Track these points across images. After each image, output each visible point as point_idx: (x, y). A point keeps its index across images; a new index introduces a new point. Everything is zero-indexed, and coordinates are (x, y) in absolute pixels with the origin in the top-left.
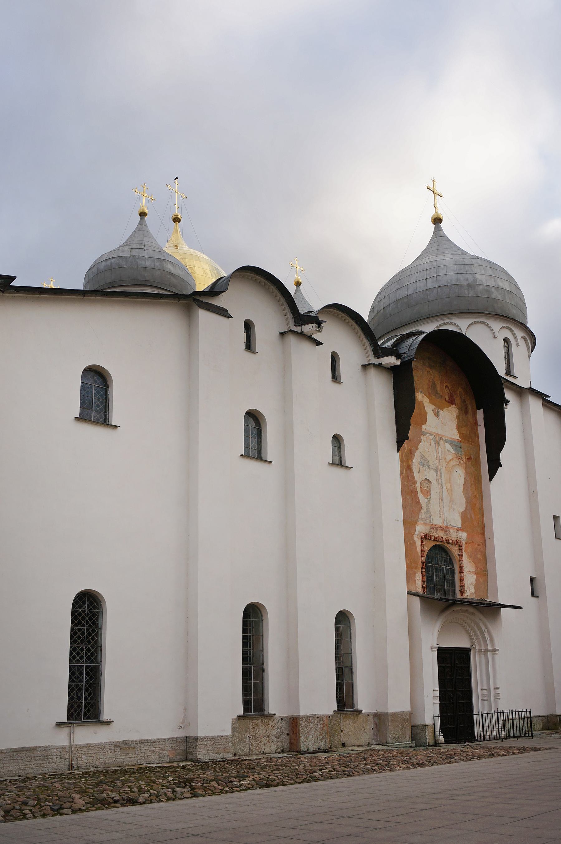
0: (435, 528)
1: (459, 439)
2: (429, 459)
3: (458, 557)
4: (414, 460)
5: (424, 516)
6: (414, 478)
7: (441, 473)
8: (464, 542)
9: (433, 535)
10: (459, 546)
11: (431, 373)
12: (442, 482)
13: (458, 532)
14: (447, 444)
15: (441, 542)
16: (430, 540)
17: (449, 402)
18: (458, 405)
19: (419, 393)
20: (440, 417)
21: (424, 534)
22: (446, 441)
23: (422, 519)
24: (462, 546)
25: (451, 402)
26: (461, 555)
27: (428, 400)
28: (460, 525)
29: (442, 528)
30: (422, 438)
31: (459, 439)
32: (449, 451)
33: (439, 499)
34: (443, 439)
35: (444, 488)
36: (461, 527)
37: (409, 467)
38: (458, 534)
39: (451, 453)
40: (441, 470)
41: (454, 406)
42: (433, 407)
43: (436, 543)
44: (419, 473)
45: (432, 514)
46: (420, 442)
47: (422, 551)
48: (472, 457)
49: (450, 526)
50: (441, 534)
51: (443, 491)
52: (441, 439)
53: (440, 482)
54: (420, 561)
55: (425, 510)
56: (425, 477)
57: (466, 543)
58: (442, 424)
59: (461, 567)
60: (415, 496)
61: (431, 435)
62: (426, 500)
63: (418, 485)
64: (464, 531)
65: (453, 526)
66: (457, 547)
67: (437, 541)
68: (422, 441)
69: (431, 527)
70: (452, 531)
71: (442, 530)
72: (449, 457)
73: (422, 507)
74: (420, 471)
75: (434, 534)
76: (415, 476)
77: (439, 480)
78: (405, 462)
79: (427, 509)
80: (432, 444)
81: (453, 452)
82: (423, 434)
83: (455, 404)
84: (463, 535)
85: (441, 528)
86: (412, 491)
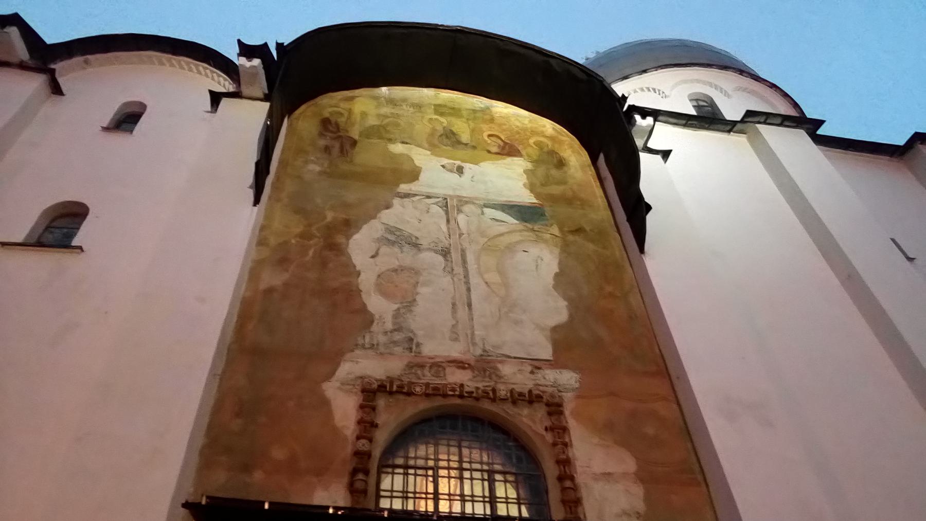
0: (428, 365)
2: (417, 234)
3: (549, 437)
4: (356, 237)
5: (382, 339)
8: (568, 397)
9: (421, 381)
10: (548, 405)
13: (536, 371)
14: (486, 210)
15: (461, 396)
16: (409, 394)
18: (529, 156)
21: (377, 380)
22: (486, 206)
23: (372, 346)
24: (560, 405)
26: (560, 430)
27: (429, 153)
28: (546, 352)
29: (462, 362)
30: (396, 202)
33: (454, 305)
35: (474, 280)
36: (552, 359)
38: (539, 375)
39: (503, 223)
43: (439, 402)
44: (373, 257)
45: (420, 333)
46: (388, 207)
47: (367, 426)
48: (588, 229)
49: (497, 357)
50: (456, 377)
52: (467, 202)
53: (459, 270)
54: (349, 450)
55: (389, 326)
56: (395, 264)
57: (578, 397)
58: (472, 181)
59: (565, 463)
61: (428, 197)
62: (396, 306)
63: (366, 281)
64: (565, 367)
65: (515, 358)
66: (540, 411)
67: (445, 396)
69: (410, 362)
70: (507, 370)
71: (464, 368)
72: (502, 229)
73: (376, 322)
75: (428, 377)
77: (455, 268)
79: (394, 324)
84: (568, 378)
85: (461, 365)
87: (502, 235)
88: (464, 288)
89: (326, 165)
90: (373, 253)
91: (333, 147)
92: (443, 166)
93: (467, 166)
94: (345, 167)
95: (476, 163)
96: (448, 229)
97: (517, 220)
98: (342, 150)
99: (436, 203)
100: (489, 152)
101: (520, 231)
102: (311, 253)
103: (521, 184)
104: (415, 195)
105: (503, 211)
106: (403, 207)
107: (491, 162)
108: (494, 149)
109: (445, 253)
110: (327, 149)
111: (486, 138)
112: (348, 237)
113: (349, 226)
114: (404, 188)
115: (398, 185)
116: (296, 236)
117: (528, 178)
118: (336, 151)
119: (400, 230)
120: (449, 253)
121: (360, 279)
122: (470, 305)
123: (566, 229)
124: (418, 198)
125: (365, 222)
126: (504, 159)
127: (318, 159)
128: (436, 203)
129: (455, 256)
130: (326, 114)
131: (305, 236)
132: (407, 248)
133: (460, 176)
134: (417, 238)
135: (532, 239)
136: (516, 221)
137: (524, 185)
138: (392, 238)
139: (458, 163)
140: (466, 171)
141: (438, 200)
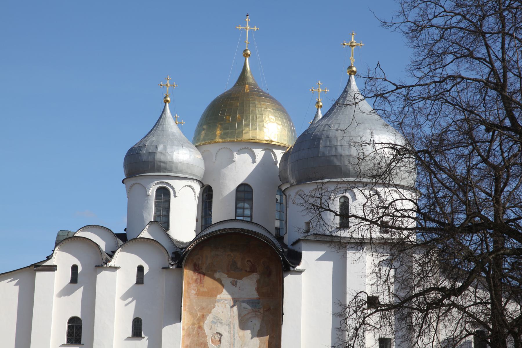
1: (258, 297)
2: (222, 318)
4: (206, 322)
6: (204, 333)
7: (234, 326)
11: (232, 255)
12: (234, 332)
17: (249, 272)
19: (218, 273)
20: (238, 285)
22: (243, 302)
25: (253, 270)
27: (227, 276)
30: (216, 304)
31: (258, 297)
32: (245, 308)
33: (230, 345)
34: (239, 301)
35: (236, 335)
37: (200, 327)
40: (234, 324)
41: (255, 274)
42: (231, 279)
44: (210, 329)
46: (214, 307)
51: (234, 338)
53: (232, 332)
60: (204, 346)
61: (226, 300)
68: (216, 307)
72: (246, 312)
74: (211, 328)
76: (206, 332)
77: (231, 331)
78: (196, 324)
80: (226, 307)
81: (249, 307)
82: (219, 301)
83: (256, 272)
86: (201, 343)
87: (245, 315)
88: (233, 338)
89: (196, 290)
90: (210, 328)
91: (198, 279)
92: (231, 282)
93: (239, 281)
94: (202, 289)
95: (241, 279)
96: (230, 314)
97: (250, 307)
98: (201, 280)
99: (227, 303)
100: (246, 271)
101: (251, 312)
102: (195, 330)
103: (254, 288)
104: (222, 300)
105: (248, 303)
106: (218, 306)
107: (246, 277)
108: (248, 269)
109: (229, 325)
110: (196, 280)
111: (246, 263)
112: (204, 322)
113: (203, 317)
114: (218, 296)
115: (216, 296)
116: (191, 325)
117: (257, 285)
118: (199, 281)
119: (217, 317)
120: (230, 325)
121: (207, 338)
122: (234, 345)
123: (265, 309)
124: (223, 301)
125: (208, 315)
126: (251, 274)
127: (194, 287)
128: (227, 303)
129: (232, 326)
130: (195, 261)
131: (193, 324)
132: (219, 325)
133: (236, 287)
134: (222, 320)
135: (254, 316)
136: (250, 308)
137: (256, 289)
138: (215, 321)
139: (236, 280)
140: (238, 283)
141: (228, 301)
